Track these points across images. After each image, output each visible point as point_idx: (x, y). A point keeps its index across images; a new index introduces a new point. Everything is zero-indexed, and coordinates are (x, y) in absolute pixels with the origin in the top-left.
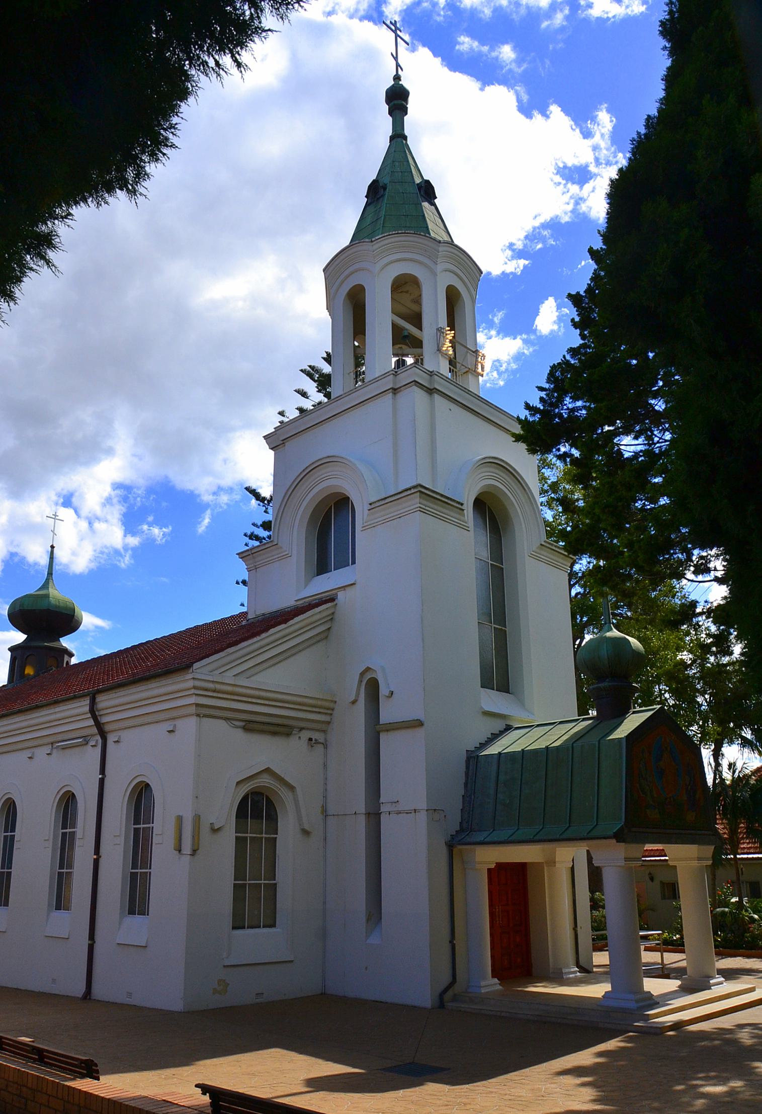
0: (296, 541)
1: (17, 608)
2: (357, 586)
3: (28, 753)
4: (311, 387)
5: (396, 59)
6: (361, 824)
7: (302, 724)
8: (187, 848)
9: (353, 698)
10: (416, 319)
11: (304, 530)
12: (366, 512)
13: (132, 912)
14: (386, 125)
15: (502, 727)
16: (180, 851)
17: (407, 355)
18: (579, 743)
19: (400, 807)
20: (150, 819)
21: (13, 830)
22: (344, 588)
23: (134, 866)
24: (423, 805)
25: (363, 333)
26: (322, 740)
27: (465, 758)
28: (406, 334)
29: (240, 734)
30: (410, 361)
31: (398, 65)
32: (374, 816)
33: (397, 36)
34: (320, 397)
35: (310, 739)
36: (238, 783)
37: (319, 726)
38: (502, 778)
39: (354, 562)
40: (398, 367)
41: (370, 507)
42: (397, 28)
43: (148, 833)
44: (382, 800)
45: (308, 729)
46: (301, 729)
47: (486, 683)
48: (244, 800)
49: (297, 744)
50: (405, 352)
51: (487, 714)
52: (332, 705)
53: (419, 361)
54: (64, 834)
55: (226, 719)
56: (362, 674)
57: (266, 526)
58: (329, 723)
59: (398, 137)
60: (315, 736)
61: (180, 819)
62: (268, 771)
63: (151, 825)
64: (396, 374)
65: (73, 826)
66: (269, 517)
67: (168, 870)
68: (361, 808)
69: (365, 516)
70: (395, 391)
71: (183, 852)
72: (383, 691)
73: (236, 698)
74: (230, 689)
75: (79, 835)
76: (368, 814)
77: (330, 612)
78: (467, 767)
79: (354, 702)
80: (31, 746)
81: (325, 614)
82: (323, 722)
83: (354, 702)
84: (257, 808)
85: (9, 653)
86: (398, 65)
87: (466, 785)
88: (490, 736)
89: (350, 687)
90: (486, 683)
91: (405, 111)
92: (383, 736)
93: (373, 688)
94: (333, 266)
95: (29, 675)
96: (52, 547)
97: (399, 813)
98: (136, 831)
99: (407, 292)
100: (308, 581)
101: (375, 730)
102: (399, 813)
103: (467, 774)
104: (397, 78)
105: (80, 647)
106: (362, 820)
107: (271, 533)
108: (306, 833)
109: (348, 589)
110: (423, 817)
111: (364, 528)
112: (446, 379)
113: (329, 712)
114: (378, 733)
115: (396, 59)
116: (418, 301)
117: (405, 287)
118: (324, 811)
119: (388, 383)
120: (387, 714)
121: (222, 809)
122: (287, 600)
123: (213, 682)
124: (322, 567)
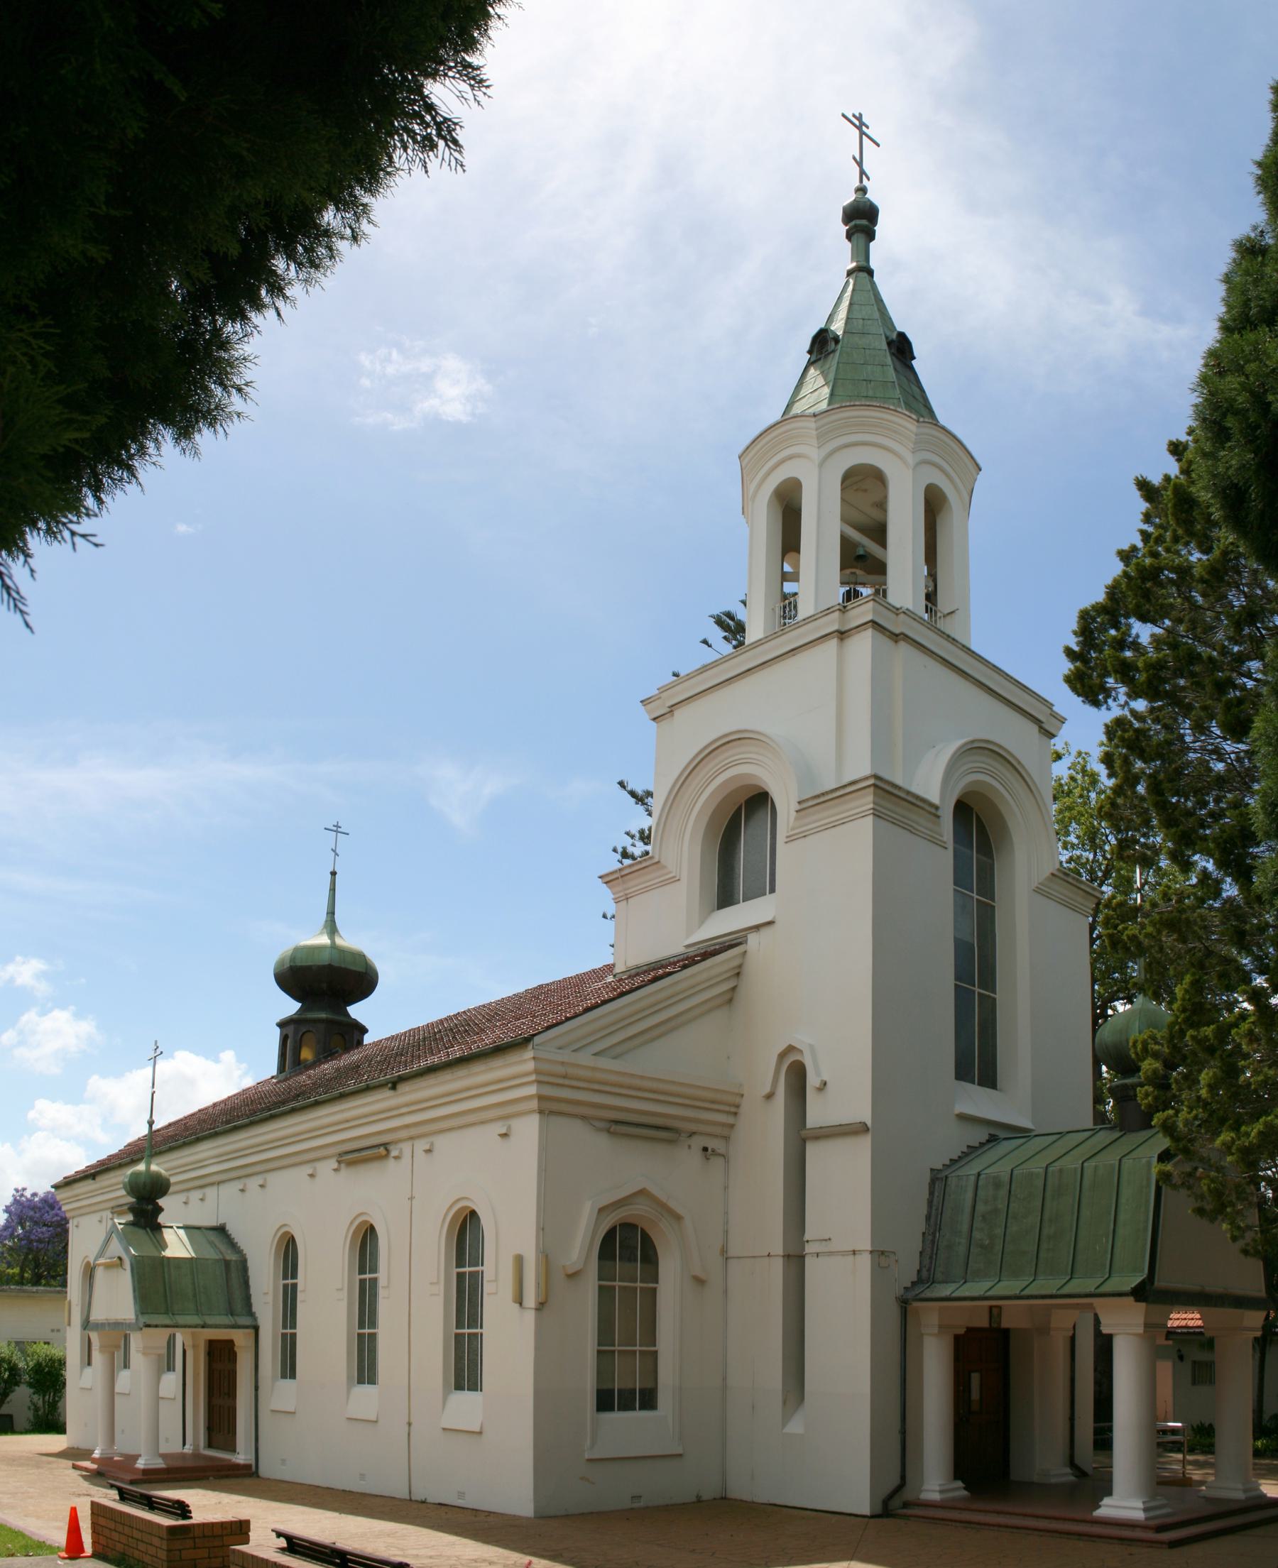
0: (686, 854)
1: (287, 965)
2: (776, 925)
3: (308, 1169)
4: (716, 634)
5: (860, 164)
6: (776, 1270)
7: (693, 1127)
8: (530, 1299)
9: (767, 1090)
10: (879, 532)
11: (698, 850)
12: (793, 814)
13: (459, 1387)
14: (842, 255)
15: (984, 1138)
16: (521, 1304)
17: (864, 584)
18: (1092, 1163)
19: (833, 1246)
20: (477, 1259)
21: (294, 1276)
22: (757, 928)
23: (459, 1324)
24: (866, 1245)
25: (797, 549)
26: (722, 1151)
27: (928, 1180)
28: (861, 552)
29: (601, 1142)
30: (866, 591)
31: (862, 173)
32: (795, 1261)
33: (862, 133)
34: (727, 648)
35: (705, 1149)
36: (600, 1210)
37: (718, 1130)
38: (981, 1208)
39: (772, 890)
40: (849, 600)
41: (798, 807)
42: (862, 124)
43: (476, 1279)
44: (807, 1237)
45: (701, 1134)
46: (692, 1134)
47: (963, 1073)
48: (610, 1236)
49: (687, 1158)
50: (859, 580)
51: (963, 1117)
52: (737, 1100)
53: (881, 593)
54: (362, 1282)
55: (584, 1118)
56: (782, 1056)
57: (645, 837)
58: (732, 1126)
59: (863, 270)
60: (712, 1144)
61: (519, 1261)
62: (642, 1192)
63: (479, 1268)
64: (843, 610)
65: (374, 1269)
66: (646, 822)
67: (509, 1334)
68: (778, 1249)
69: (792, 819)
70: (842, 635)
71: (525, 1303)
72: (812, 1081)
73: (596, 1087)
74: (588, 1074)
75: (382, 1282)
76: (787, 1257)
77: (736, 963)
78: (931, 1193)
79: (769, 1096)
80: (310, 1159)
81: (726, 967)
82: (723, 1125)
83: (769, 1096)
84: (627, 1247)
85: (278, 1030)
86: (862, 173)
87: (928, 1218)
88: (965, 1150)
89: (763, 1074)
90: (963, 1073)
91: (871, 236)
92: (812, 1149)
93: (797, 1075)
94: (753, 452)
95: (306, 1060)
96: (334, 874)
97: (831, 1253)
98: (460, 1277)
99: (865, 491)
100: (703, 920)
101: (800, 1137)
102: (831, 1253)
103: (930, 1203)
104: (862, 190)
105: (379, 1018)
106: (778, 1265)
107: (648, 848)
108: (700, 1282)
109: (764, 931)
110: (865, 1262)
111: (790, 839)
112: (920, 620)
113: (733, 1110)
114: (804, 1141)
115: (860, 164)
116: (882, 505)
117: (864, 484)
118: (724, 1251)
119: (832, 623)
120: (818, 1113)
121: (579, 1247)
122: (673, 944)
123: (563, 1063)
124: (726, 897)
